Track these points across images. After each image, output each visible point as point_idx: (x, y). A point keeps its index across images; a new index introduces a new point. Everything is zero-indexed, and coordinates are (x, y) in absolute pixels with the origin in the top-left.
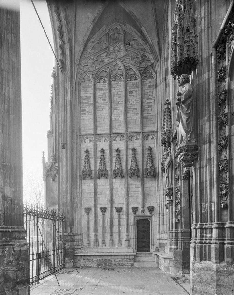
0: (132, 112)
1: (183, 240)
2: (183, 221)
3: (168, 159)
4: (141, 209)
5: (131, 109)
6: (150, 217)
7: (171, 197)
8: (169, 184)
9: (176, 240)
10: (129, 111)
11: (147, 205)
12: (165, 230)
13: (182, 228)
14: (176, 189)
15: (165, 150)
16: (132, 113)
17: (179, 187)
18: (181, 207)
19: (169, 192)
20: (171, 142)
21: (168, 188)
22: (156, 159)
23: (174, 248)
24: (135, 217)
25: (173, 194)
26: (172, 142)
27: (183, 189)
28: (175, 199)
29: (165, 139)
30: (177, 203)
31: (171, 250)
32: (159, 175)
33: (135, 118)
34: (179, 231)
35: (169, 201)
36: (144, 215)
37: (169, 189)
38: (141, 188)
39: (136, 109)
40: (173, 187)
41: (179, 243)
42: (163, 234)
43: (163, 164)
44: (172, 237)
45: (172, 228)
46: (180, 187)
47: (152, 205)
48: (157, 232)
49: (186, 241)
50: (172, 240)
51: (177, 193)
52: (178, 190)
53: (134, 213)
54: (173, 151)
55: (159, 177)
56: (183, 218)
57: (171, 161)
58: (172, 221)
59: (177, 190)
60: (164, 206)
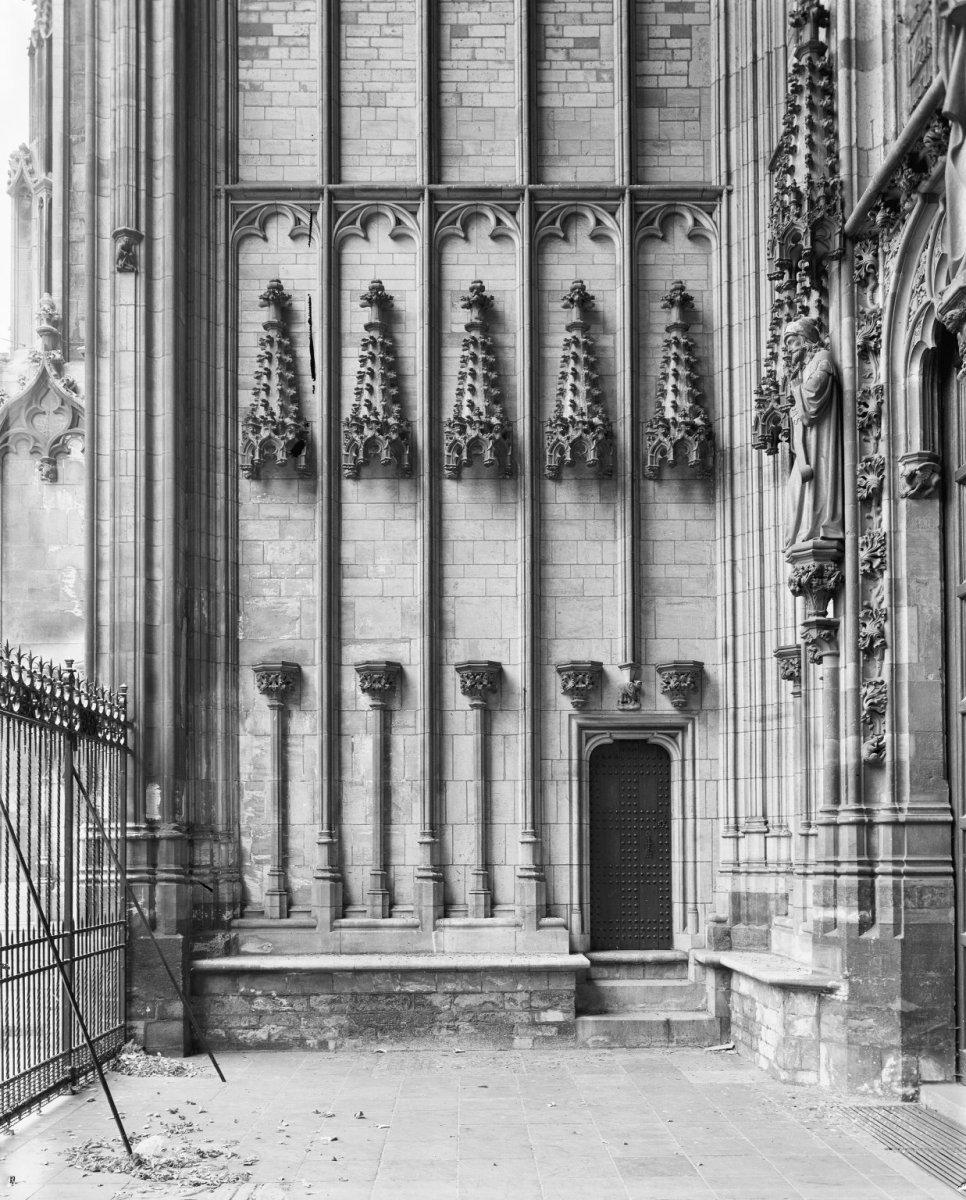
0: (569, 59)
1: (908, 874)
2: (906, 756)
3: (814, 368)
4: (621, 678)
5: (562, 43)
6: (675, 730)
7: (831, 601)
8: (816, 518)
9: (860, 874)
10: (550, 54)
11: (664, 651)
12: (772, 812)
13: (897, 796)
14: (864, 555)
15: (779, 305)
16: (567, 65)
17: (883, 543)
18: (895, 669)
19: (819, 573)
20: (833, 258)
21: (810, 543)
22: (720, 363)
23: (849, 925)
24: (581, 728)
25: (841, 582)
26: (841, 257)
27: (909, 554)
28: (856, 613)
29: (797, 238)
30: (872, 642)
31: (834, 933)
32: (737, 468)
33: (590, 100)
34: (882, 816)
35: (820, 625)
37: (817, 553)
38: (620, 542)
39: (593, 43)
40: (842, 541)
41: (884, 889)
42: (758, 839)
43: (770, 393)
44: (836, 853)
45: (837, 800)
46: (888, 542)
47: (691, 656)
48: (722, 823)
49: (927, 881)
51: (871, 576)
52: (877, 562)
54: (845, 310)
55: (737, 478)
56: (906, 739)
57: (831, 382)
58: (836, 753)
59: (869, 562)
60: (763, 659)
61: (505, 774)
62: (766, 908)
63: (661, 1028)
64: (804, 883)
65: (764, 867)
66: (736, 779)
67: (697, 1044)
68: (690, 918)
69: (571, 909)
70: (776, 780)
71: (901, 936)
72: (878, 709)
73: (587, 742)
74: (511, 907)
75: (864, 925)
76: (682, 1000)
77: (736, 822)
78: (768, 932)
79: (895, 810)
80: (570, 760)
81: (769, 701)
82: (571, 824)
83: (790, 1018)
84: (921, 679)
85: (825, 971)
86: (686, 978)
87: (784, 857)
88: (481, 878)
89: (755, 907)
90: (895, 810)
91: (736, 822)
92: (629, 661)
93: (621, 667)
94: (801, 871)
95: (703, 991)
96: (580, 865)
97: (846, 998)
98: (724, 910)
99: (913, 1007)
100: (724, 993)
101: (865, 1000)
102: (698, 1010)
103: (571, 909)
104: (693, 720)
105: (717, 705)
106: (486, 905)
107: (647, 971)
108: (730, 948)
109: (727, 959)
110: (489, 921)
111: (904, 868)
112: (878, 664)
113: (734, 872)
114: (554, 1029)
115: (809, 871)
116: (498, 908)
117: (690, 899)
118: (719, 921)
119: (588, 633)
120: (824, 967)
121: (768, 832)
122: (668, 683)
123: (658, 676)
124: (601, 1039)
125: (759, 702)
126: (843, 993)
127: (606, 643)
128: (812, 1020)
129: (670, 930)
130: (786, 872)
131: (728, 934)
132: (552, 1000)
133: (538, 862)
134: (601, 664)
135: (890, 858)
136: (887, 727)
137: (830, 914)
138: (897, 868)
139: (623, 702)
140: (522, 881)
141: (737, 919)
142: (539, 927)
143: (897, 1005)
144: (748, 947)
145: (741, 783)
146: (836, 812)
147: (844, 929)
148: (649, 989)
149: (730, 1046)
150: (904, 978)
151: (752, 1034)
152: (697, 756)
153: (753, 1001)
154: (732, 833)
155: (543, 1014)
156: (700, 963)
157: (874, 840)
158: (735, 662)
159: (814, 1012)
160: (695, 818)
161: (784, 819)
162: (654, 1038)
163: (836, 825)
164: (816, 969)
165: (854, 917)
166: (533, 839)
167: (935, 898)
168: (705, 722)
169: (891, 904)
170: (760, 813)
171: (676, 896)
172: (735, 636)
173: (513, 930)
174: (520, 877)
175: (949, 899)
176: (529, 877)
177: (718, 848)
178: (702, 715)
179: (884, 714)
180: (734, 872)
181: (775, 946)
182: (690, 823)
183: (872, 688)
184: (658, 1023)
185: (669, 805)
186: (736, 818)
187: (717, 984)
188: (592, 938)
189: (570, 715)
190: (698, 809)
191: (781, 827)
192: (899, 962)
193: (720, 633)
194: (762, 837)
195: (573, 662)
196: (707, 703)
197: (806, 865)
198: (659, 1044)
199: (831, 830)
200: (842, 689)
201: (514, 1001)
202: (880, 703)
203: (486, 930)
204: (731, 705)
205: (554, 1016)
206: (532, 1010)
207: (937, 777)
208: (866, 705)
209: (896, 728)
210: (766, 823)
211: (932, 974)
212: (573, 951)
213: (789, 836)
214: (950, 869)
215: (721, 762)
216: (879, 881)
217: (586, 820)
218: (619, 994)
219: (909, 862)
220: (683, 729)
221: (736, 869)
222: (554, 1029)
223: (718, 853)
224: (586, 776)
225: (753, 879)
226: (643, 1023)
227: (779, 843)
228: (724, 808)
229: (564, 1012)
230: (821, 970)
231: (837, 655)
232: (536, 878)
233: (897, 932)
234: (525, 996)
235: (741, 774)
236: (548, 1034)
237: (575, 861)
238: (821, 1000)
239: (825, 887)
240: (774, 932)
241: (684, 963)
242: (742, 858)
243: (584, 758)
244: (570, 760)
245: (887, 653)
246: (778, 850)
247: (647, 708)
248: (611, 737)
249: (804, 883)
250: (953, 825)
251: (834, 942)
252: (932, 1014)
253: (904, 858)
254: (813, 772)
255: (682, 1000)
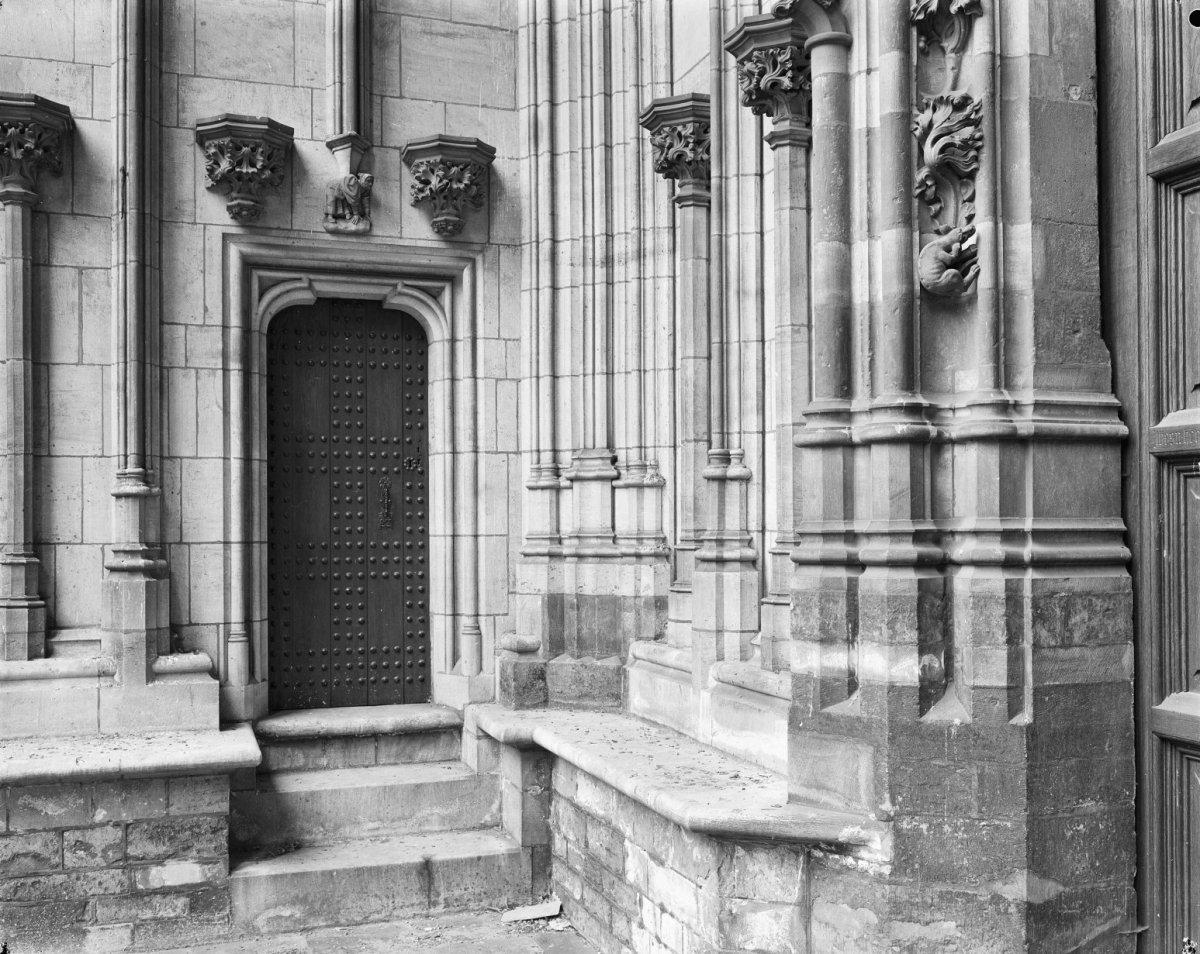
1: (1039, 563)
2: (1023, 280)
4: (330, 168)
6: (437, 281)
9: (920, 564)
12: (626, 440)
13: (1003, 373)
18: (999, 67)
23: (894, 690)
24: (248, 265)
31: (850, 707)
36: (358, 253)
42: (597, 492)
44: (849, 514)
47: (463, 128)
48: (527, 462)
49: (1079, 580)
50: (854, 564)
53: (236, 213)
61: (81, 352)
62: (614, 624)
63: (414, 876)
64: (719, 581)
65: (608, 548)
66: (555, 377)
67: (485, 903)
68: (466, 644)
69: (227, 634)
70: (633, 378)
71: (1025, 718)
72: (961, 161)
73: (261, 295)
74: (93, 634)
75: (930, 691)
76: (453, 809)
77: (555, 460)
78: (621, 673)
79: (1004, 407)
80: (225, 327)
81: (618, 227)
82: (226, 459)
83: (735, 906)
84: (1056, 95)
85: (824, 798)
86: (457, 759)
87: (650, 525)
88: (21, 573)
89: (594, 624)
90: (1004, 407)
91: (555, 460)
92: (348, 130)
93: (331, 145)
94: (712, 554)
95: (494, 791)
96: (247, 543)
97: (887, 870)
98: (532, 632)
99: (1051, 889)
100: (538, 797)
101: (933, 875)
102: (484, 827)
103: (227, 634)
104: (473, 262)
105: (520, 238)
106: (31, 633)
107: (383, 748)
108: (545, 703)
109: (547, 729)
110: (40, 665)
111: (1029, 550)
112: (950, 59)
113: (551, 555)
114: (182, 902)
115: (727, 555)
116: (64, 635)
117: (466, 607)
118: (524, 651)
119: (265, 72)
120: (820, 787)
121: (618, 478)
122: (427, 182)
123: (405, 170)
124: (286, 913)
125: (600, 228)
126: (877, 853)
127: (300, 93)
128: (789, 913)
129: (426, 665)
130: (656, 556)
131: (541, 674)
132: (175, 839)
133: (153, 536)
134: (290, 131)
135: (909, 527)
136: (981, 205)
137: (837, 659)
138: (1013, 549)
139: (337, 217)
140: (116, 578)
141: (557, 645)
142: (152, 675)
143: (1017, 888)
144: (581, 700)
145: (564, 385)
146: (846, 416)
147: (882, 698)
148: (389, 791)
149: (552, 907)
150: (1033, 821)
151: (612, 904)
152: (480, 333)
153: (617, 834)
154: (546, 480)
155: (154, 871)
156: (488, 736)
157: (945, 482)
158: (553, 154)
159: (795, 893)
160: (476, 451)
161: (650, 452)
162: (399, 901)
163: (848, 445)
164: (802, 792)
165: (908, 669)
166: (141, 488)
167: (1095, 623)
168: (495, 267)
169: (1002, 638)
170: (601, 442)
171: (438, 602)
172: (553, 104)
173: (91, 685)
174: (113, 570)
175: (1122, 623)
176: (132, 571)
177: (520, 510)
178: (490, 254)
179: (972, 176)
180: (551, 555)
181: (636, 700)
182: (465, 461)
183: (944, 112)
184: (405, 870)
185: (424, 428)
186: (555, 451)
187: (525, 782)
188: (272, 686)
189: (225, 237)
190: (481, 434)
191: (643, 467)
192: (1021, 780)
193: (524, 100)
194: (607, 486)
195: (228, 118)
196: (499, 233)
197: (720, 542)
198: (409, 912)
199: (838, 456)
200: (859, 122)
201: (86, 847)
202: (966, 145)
203: (29, 688)
204: (545, 233)
205: (184, 872)
206: (127, 863)
207: (1087, 332)
208: (931, 153)
209: (1002, 211)
210: (614, 460)
211: (1089, 805)
212: (228, 721)
213: (660, 486)
214: (1120, 550)
215: (526, 346)
216: (963, 581)
217: (259, 452)
218: (326, 806)
219: (1039, 535)
220: (453, 280)
221: (556, 549)
222: (182, 902)
223: (519, 517)
224: (259, 365)
225: (589, 569)
226: (375, 872)
227: (640, 499)
228: (531, 431)
229: (203, 862)
230: (813, 794)
231: (845, 44)
232: (146, 571)
233: (1014, 709)
234: (113, 835)
235: (564, 367)
236: (167, 913)
237: (236, 534)
238: (812, 867)
239: (826, 596)
240: (635, 675)
241: (455, 730)
242: (566, 528)
243: (255, 325)
244: (225, 327)
245: (981, 27)
246: (637, 513)
247: (384, 232)
248: (310, 287)
249: (719, 581)
250: (1124, 445)
251: (852, 730)
252: (1091, 900)
253: (1028, 524)
254: (734, 348)
255: (453, 809)
